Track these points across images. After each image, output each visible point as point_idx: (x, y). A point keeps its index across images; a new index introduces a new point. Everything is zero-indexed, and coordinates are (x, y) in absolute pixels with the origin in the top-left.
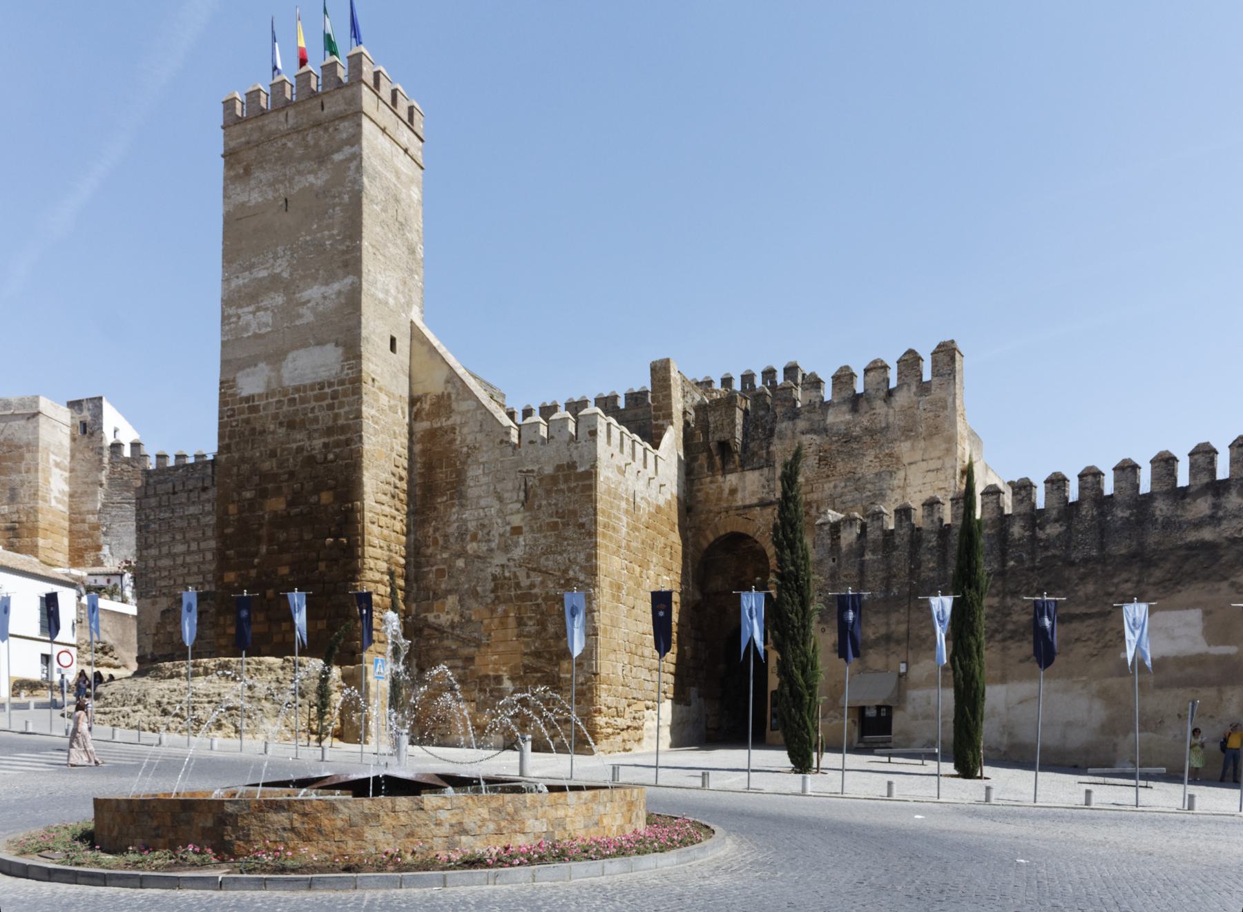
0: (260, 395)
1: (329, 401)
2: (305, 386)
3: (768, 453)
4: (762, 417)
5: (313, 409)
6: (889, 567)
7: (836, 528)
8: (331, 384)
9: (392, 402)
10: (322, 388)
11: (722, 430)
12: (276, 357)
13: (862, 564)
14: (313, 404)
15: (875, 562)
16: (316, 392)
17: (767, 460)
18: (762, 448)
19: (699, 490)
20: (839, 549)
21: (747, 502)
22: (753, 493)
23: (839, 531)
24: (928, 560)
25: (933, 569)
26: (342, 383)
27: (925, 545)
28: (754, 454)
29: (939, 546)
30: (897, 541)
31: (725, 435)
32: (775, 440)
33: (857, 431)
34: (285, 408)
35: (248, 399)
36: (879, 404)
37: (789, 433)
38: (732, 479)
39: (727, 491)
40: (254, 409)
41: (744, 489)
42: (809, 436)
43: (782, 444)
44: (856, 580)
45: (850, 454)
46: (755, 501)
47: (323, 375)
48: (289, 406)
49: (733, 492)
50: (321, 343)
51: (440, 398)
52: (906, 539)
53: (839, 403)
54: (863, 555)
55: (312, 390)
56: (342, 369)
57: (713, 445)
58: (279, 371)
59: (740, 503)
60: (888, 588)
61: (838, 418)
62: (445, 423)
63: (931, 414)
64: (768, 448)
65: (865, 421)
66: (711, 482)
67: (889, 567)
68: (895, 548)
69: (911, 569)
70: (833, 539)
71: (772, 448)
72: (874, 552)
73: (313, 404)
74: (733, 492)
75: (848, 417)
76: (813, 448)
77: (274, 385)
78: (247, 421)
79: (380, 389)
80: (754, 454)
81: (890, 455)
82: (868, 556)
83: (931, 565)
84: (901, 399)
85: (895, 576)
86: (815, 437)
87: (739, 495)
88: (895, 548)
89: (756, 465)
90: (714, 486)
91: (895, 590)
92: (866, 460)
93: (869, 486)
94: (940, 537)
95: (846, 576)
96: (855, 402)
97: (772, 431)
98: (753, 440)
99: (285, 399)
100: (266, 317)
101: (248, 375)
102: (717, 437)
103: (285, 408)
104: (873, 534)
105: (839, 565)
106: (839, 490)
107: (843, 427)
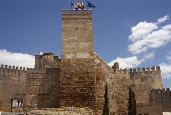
5: (83, 63)
7: (157, 91)
8: (87, 59)
12: (75, 53)
13: (162, 96)
20: (158, 94)
32: (134, 76)
35: (68, 59)
40: (70, 61)
47: (86, 57)
48: (78, 61)
51: (99, 64)
56: (90, 57)
60: (167, 100)
61: (143, 74)
62: (99, 68)
75: (145, 74)
78: (68, 63)
82: (163, 95)
84: (153, 73)
88: (167, 94)
91: (168, 100)
96: (146, 72)
97: (133, 75)
100: (73, 46)
101: (68, 55)
103: (77, 62)
104: (163, 92)
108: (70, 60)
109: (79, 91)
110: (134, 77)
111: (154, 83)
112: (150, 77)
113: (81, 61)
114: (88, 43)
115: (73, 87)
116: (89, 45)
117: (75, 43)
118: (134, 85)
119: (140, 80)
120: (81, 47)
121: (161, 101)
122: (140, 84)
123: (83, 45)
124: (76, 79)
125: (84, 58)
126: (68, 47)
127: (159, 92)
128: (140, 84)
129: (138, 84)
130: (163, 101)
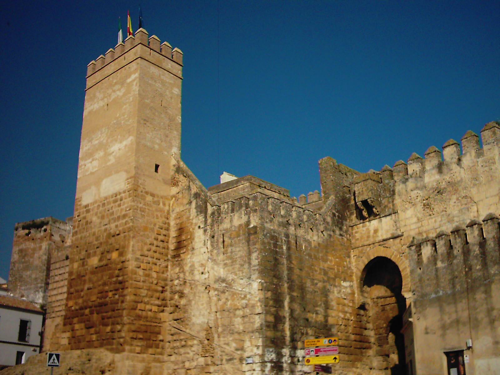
0: (91, 203)
1: (119, 202)
2: (109, 196)
3: (393, 205)
4: (388, 184)
6: (452, 271)
8: (120, 193)
9: (156, 199)
10: (116, 196)
11: (363, 194)
12: (98, 183)
13: (437, 270)
14: (112, 205)
15: (445, 268)
16: (114, 198)
17: (393, 210)
18: (389, 203)
19: (356, 232)
21: (385, 237)
22: (387, 231)
23: (420, 250)
24: (476, 265)
25: (480, 270)
26: (124, 192)
27: (472, 254)
28: (386, 207)
29: (481, 253)
30: (455, 252)
31: (365, 197)
32: (397, 197)
33: (443, 185)
34: (101, 209)
36: (454, 167)
37: (404, 191)
38: (374, 224)
39: (372, 232)
41: (382, 229)
42: (416, 192)
43: (401, 198)
44: (435, 282)
45: (442, 200)
46: (389, 236)
48: (102, 207)
49: (376, 231)
50: (117, 172)
52: (460, 251)
53: (430, 169)
54: (436, 264)
55: (112, 197)
57: (359, 204)
58: (99, 190)
59: (380, 238)
60: (454, 286)
63: (486, 169)
64: (393, 201)
65: (447, 178)
66: (363, 227)
67: (452, 271)
68: (455, 257)
69: (466, 272)
70: (419, 255)
71: (395, 202)
72: (443, 261)
73: (112, 205)
74: (376, 231)
75: (437, 177)
76: (419, 198)
77: (97, 198)
79: (147, 193)
80: (386, 207)
81: (466, 197)
82: (440, 264)
83: (478, 267)
85: (457, 277)
86: (419, 192)
87: (379, 234)
88: (455, 257)
89: (387, 213)
90: (364, 229)
91: (458, 287)
92: (452, 203)
93: (456, 219)
94: (480, 247)
95: (428, 280)
97: (393, 193)
98: (384, 198)
99: (101, 204)
102: (360, 199)
105: (423, 272)
106: (438, 224)
107: (435, 184)
108: (89, 207)
109: (94, 298)
110: (398, 200)
111: (475, 208)
112: (453, 185)
113: (109, 203)
114: (124, 143)
115: (86, 287)
116: (126, 146)
117: (101, 154)
118: (398, 237)
119: (420, 207)
120: (112, 160)
121: (433, 296)
122: (419, 224)
123: (114, 154)
124: (94, 261)
125: (115, 192)
126: (89, 168)
127: (427, 251)
128: (419, 224)
129: (413, 227)
130: (441, 293)
